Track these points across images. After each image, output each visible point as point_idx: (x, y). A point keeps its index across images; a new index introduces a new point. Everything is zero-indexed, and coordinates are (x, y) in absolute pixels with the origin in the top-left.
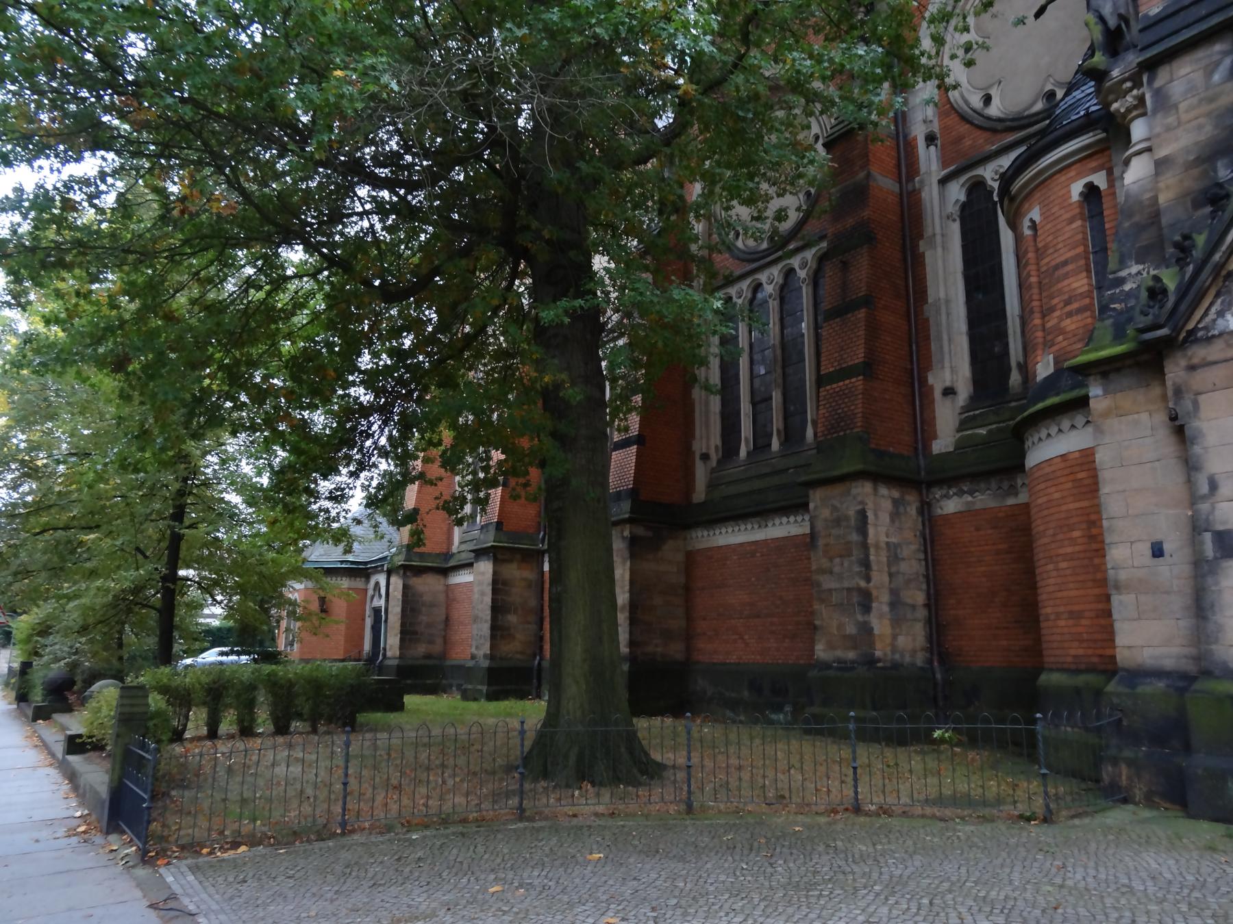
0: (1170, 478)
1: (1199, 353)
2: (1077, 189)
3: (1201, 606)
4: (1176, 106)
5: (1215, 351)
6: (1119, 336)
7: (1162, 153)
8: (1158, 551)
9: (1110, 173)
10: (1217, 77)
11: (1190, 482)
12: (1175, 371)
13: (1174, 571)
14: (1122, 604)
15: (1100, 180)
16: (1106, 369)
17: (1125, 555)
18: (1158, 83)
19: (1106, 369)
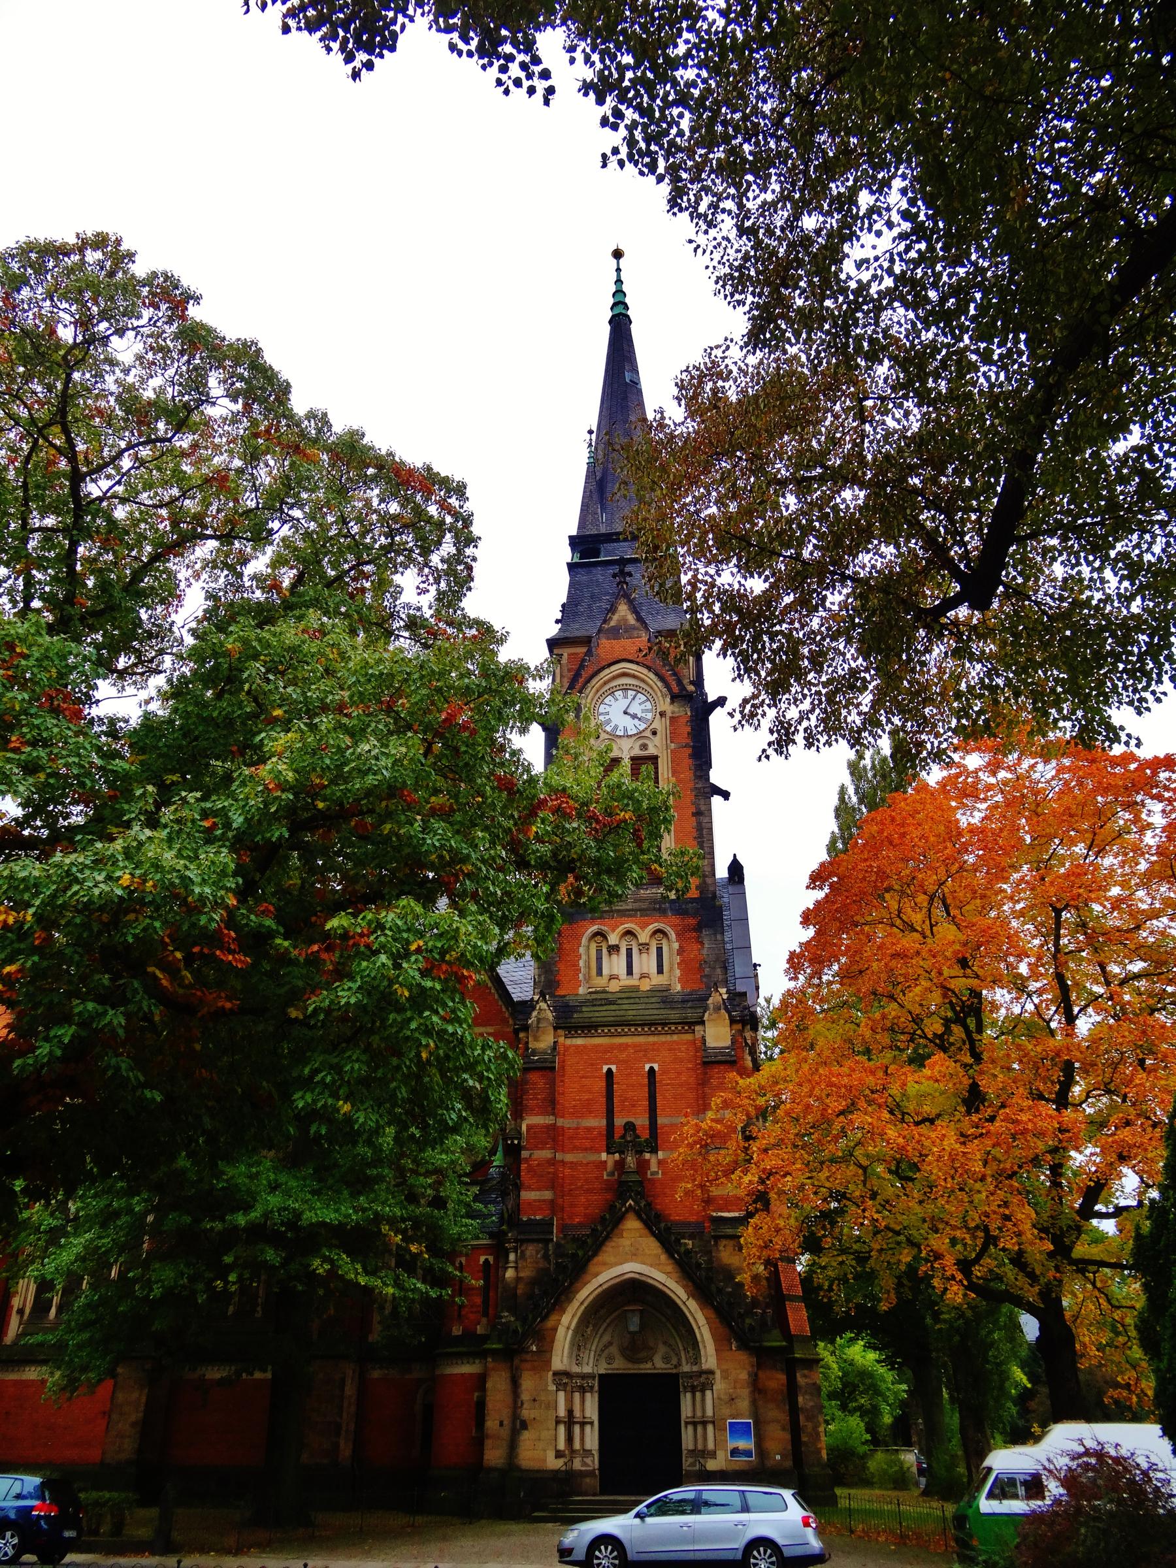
0: (509, 1399)
1: (525, 1356)
2: (482, 1259)
3: (513, 1445)
5: (528, 1357)
6: (499, 1342)
7: (522, 1275)
8: (501, 1424)
9: (496, 1259)
11: (515, 1402)
12: (516, 1362)
13: (505, 1432)
14: (488, 1443)
15: (491, 1259)
16: (494, 1353)
17: (491, 1424)
19: (494, 1353)
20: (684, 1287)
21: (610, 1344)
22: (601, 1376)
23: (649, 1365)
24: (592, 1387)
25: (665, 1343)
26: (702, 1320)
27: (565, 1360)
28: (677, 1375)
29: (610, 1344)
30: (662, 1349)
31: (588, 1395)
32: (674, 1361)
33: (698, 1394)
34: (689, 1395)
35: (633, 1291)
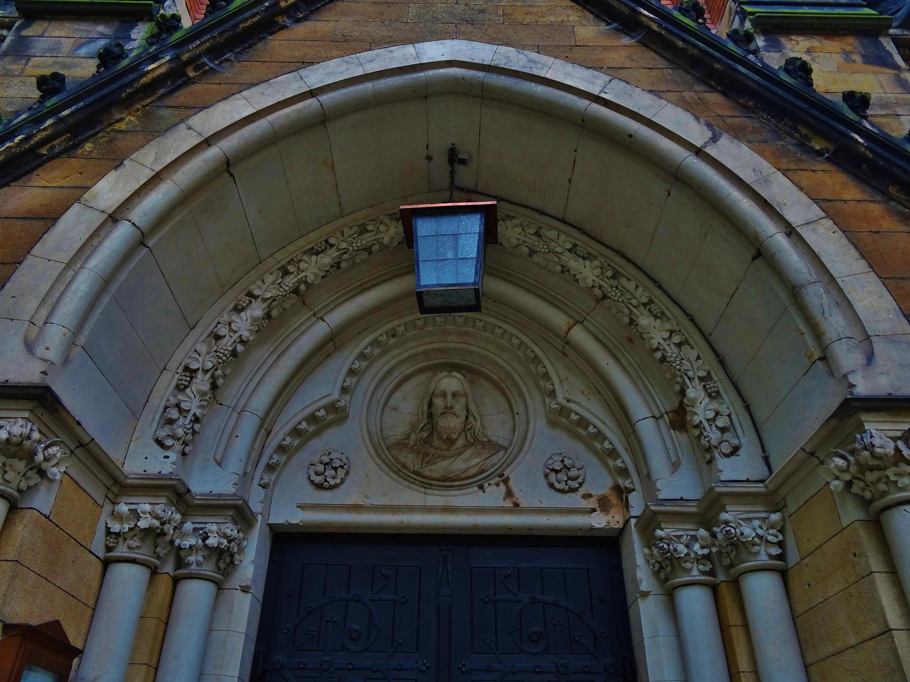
4: (29, 58)
10: (83, 51)
18: (24, 33)
20: (686, 105)
21: (336, 414)
22: (284, 540)
23: (494, 495)
24: (225, 558)
25: (560, 418)
26: (798, 208)
27: (54, 339)
28: (609, 544)
29: (336, 414)
30: (545, 442)
31: (196, 594)
32: (600, 483)
33: (763, 591)
34: (695, 603)
35: (456, 151)
